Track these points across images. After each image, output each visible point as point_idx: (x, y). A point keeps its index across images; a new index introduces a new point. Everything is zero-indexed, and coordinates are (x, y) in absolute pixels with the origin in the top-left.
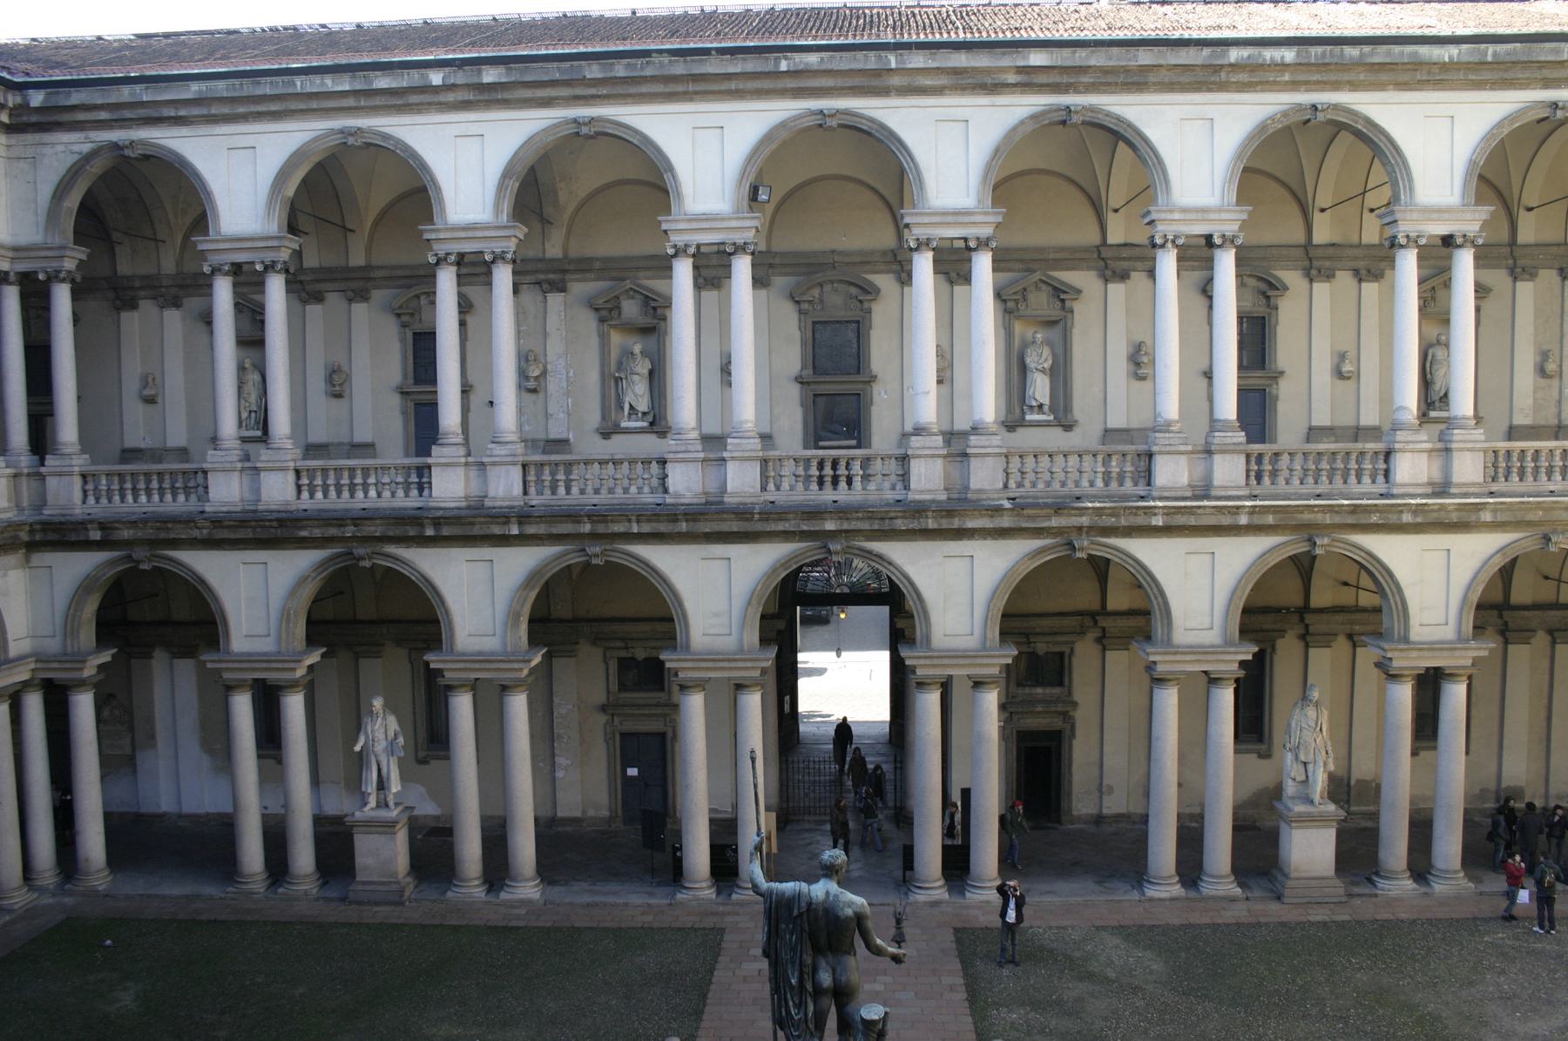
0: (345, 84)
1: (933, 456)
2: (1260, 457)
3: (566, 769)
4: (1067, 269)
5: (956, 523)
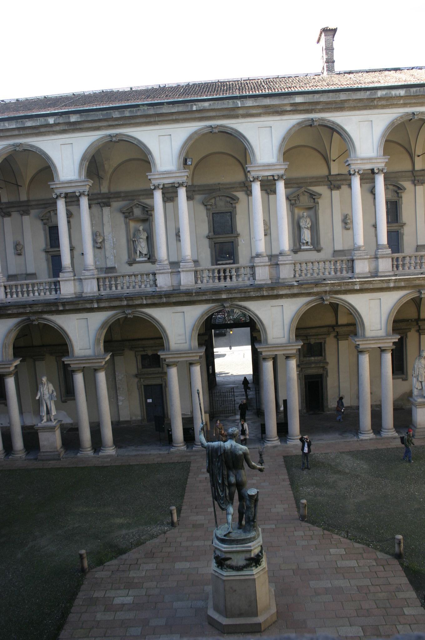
1: (264, 266)
2: (397, 258)
4: (315, 186)
5: (275, 292)
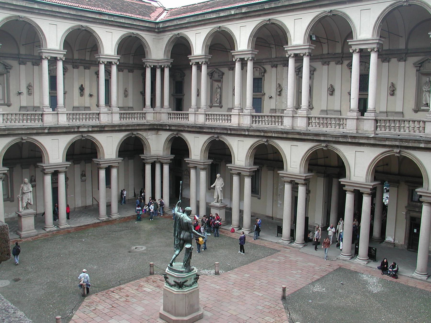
0: (214, 16)
1: (353, 119)
3: (280, 204)
5: (357, 141)
